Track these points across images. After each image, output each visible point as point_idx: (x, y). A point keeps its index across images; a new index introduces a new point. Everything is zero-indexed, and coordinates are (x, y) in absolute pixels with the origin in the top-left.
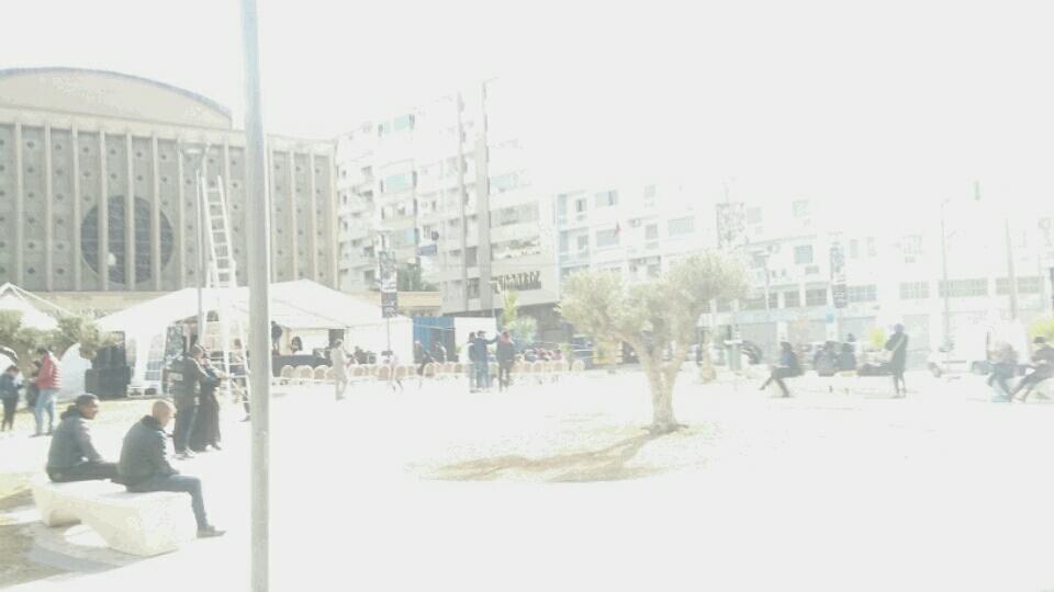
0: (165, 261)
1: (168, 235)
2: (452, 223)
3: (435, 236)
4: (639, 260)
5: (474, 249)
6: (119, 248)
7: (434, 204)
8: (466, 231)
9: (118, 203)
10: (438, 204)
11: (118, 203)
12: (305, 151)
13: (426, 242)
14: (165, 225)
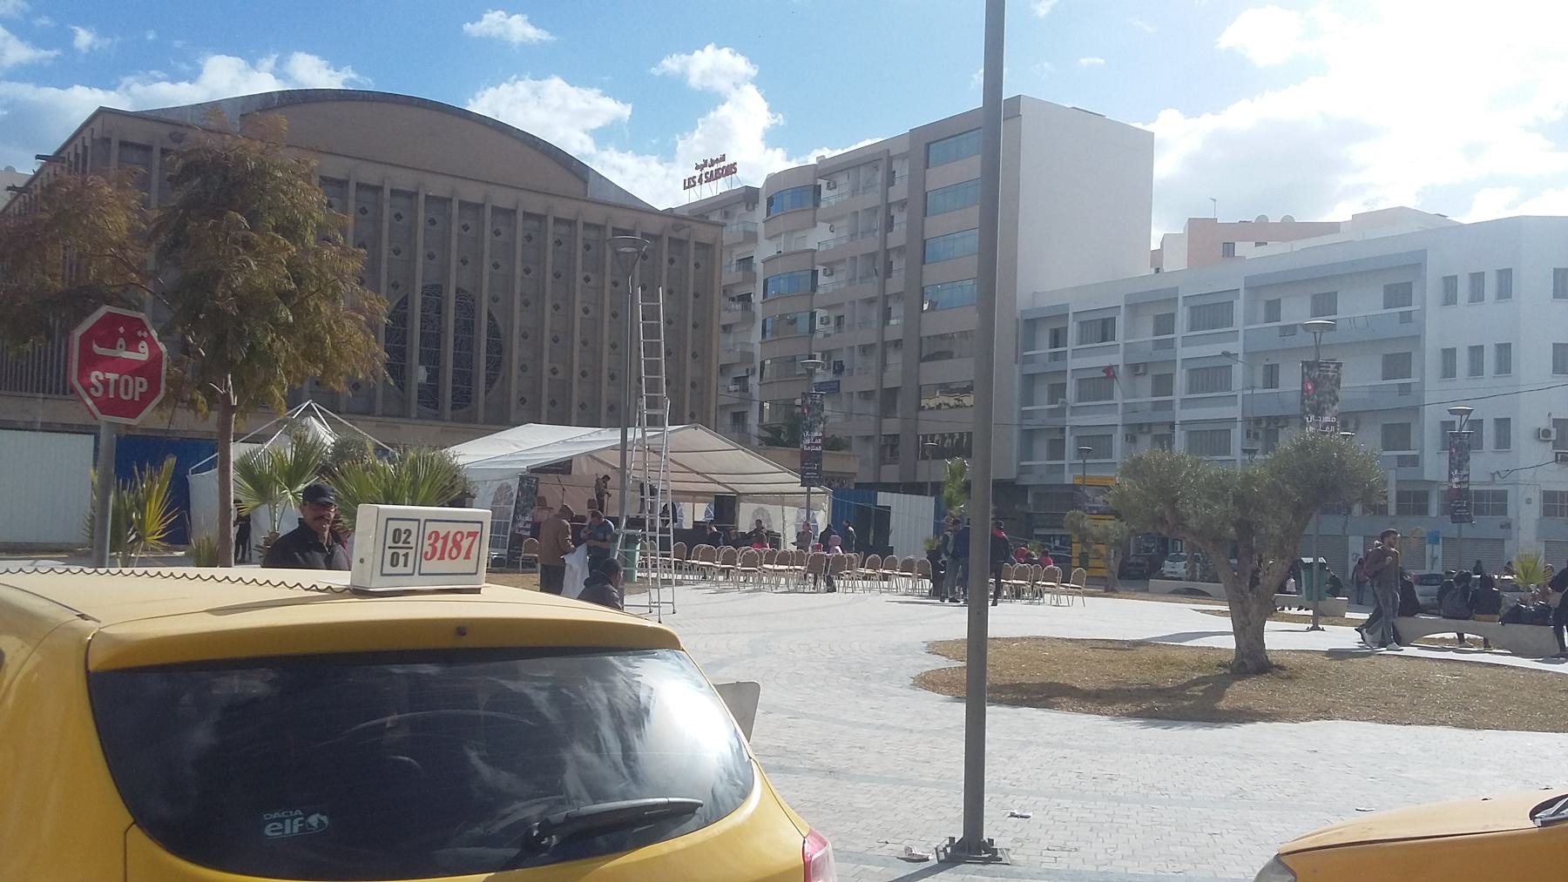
0: (490, 382)
1: (497, 348)
2: (865, 349)
3: (839, 368)
4: (1141, 425)
5: (892, 393)
6: (432, 359)
7: (839, 319)
8: (884, 365)
9: (434, 293)
10: (846, 320)
11: (434, 293)
12: (682, 235)
13: (823, 375)
14: (493, 330)
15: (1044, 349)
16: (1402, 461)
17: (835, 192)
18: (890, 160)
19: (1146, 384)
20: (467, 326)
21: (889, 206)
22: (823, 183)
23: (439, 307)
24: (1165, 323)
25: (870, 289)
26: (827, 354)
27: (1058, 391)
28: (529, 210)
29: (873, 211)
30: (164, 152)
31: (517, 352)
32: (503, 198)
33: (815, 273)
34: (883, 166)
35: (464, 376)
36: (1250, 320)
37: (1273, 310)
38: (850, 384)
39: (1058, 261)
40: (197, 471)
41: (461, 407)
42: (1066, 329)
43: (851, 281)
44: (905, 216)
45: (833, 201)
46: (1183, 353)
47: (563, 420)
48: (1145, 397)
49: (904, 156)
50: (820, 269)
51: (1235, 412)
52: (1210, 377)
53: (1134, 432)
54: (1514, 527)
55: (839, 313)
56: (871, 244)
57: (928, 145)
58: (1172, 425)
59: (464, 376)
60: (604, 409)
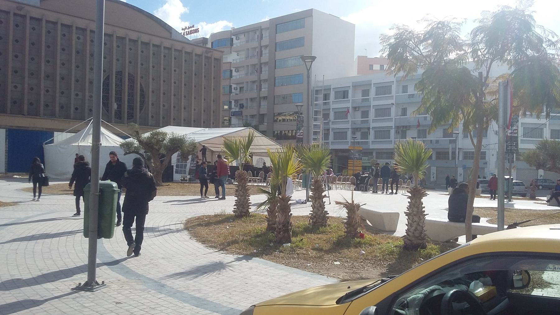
0: (141, 110)
1: (143, 95)
2: (252, 100)
3: (242, 106)
4: (357, 129)
5: (262, 116)
6: (119, 100)
7: (241, 88)
8: (260, 106)
9: (120, 74)
10: (244, 89)
11: (120, 74)
12: (209, 55)
13: (235, 109)
14: (142, 90)
15: (321, 102)
16: (451, 142)
17: (239, 41)
18: (262, 30)
19: (359, 114)
20: (132, 87)
21: (261, 47)
22: (234, 37)
23: (121, 80)
24: (366, 93)
25: (254, 77)
26: (237, 101)
27: (326, 116)
28: (155, 43)
29: (254, 49)
30: (15, 14)
31: (151, 98)
32: (145, 38)
33: (231, 71)
34: (258, 33)
35: (131, 108)
36: (397, 92)
37: (405, 89)
38: (246, 112)
39: (332, 68)
40: (46, 144)
41: (130, 119)
42: (329, 94)
43: (247, 74)
44: (267, 51)
45: (239, 45)
46: (373, 103)
47: (189, 126)
48: (359, 119)
49: (268, 28)
50: (233, 70)
51: (392, 124)
52: (383, 112)
53: (355, 130)
54: (488, 163)
55: (241, 86)
56: (255, 61)
57: (277, 25)
58: (369, 128)
59: (131, 108)
60: (182, 121)
